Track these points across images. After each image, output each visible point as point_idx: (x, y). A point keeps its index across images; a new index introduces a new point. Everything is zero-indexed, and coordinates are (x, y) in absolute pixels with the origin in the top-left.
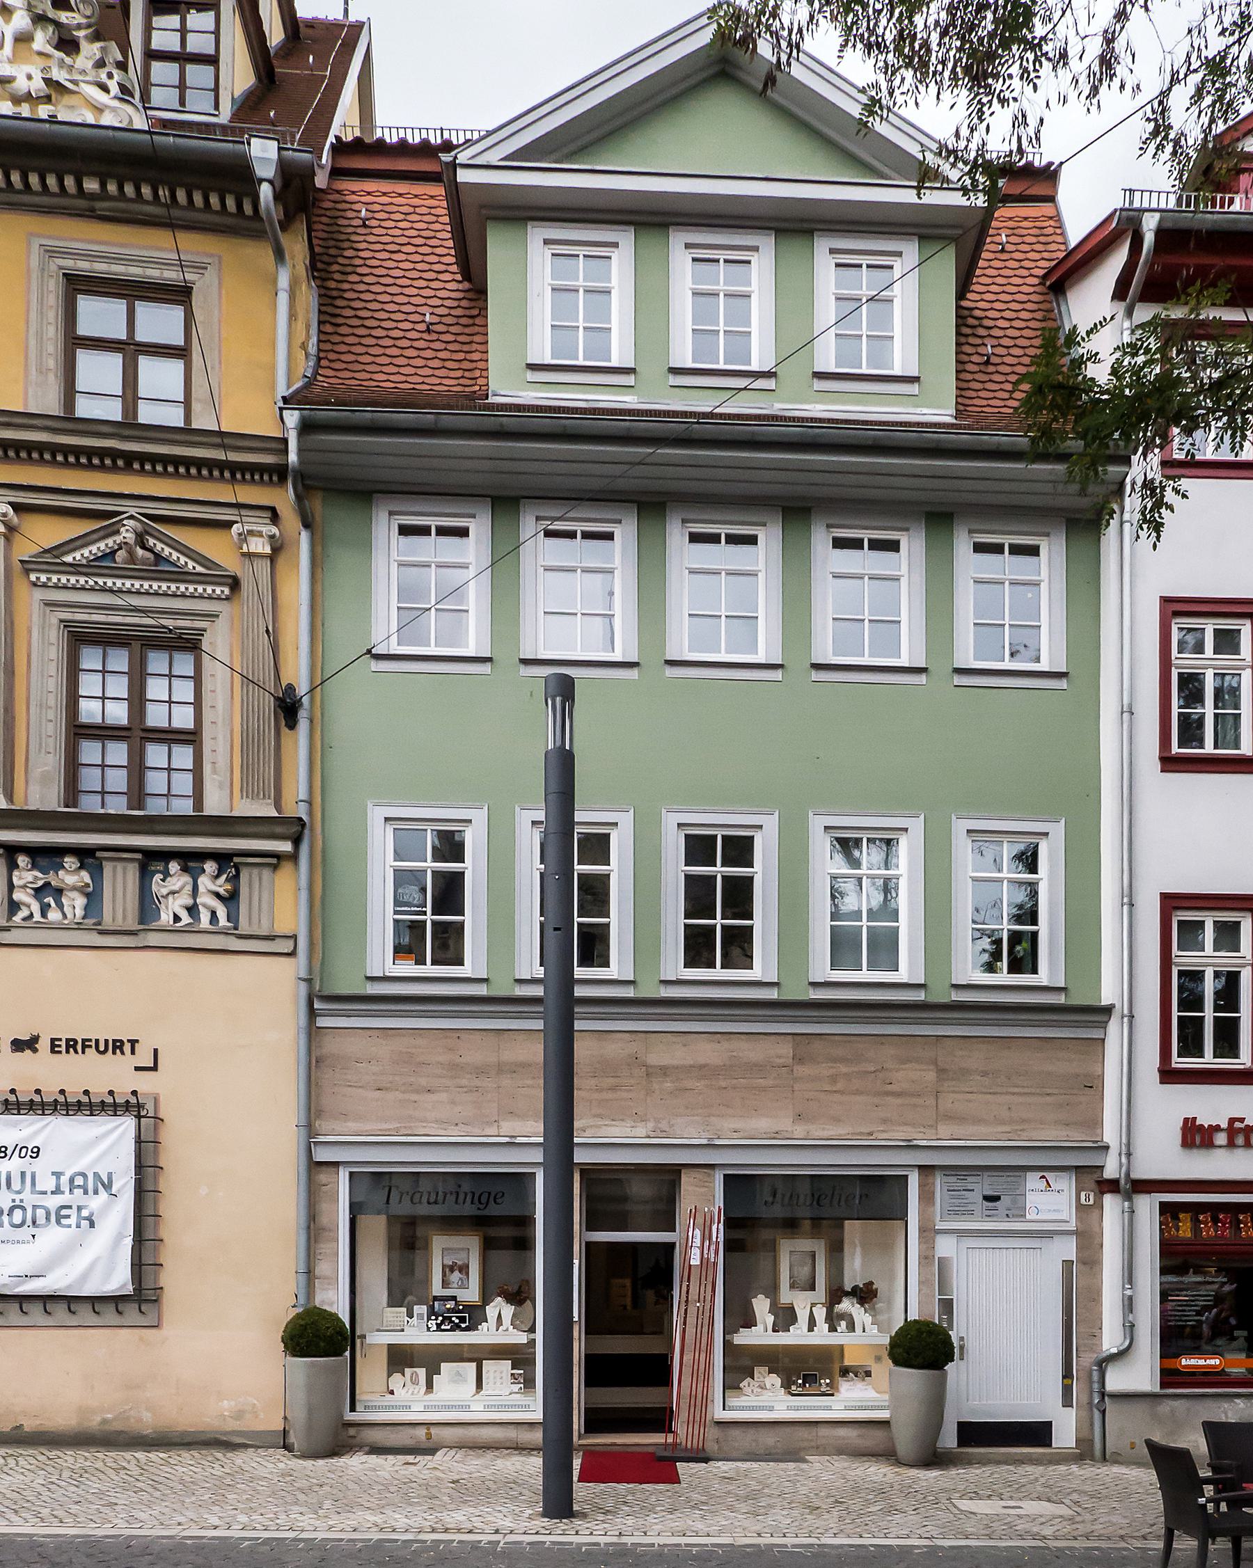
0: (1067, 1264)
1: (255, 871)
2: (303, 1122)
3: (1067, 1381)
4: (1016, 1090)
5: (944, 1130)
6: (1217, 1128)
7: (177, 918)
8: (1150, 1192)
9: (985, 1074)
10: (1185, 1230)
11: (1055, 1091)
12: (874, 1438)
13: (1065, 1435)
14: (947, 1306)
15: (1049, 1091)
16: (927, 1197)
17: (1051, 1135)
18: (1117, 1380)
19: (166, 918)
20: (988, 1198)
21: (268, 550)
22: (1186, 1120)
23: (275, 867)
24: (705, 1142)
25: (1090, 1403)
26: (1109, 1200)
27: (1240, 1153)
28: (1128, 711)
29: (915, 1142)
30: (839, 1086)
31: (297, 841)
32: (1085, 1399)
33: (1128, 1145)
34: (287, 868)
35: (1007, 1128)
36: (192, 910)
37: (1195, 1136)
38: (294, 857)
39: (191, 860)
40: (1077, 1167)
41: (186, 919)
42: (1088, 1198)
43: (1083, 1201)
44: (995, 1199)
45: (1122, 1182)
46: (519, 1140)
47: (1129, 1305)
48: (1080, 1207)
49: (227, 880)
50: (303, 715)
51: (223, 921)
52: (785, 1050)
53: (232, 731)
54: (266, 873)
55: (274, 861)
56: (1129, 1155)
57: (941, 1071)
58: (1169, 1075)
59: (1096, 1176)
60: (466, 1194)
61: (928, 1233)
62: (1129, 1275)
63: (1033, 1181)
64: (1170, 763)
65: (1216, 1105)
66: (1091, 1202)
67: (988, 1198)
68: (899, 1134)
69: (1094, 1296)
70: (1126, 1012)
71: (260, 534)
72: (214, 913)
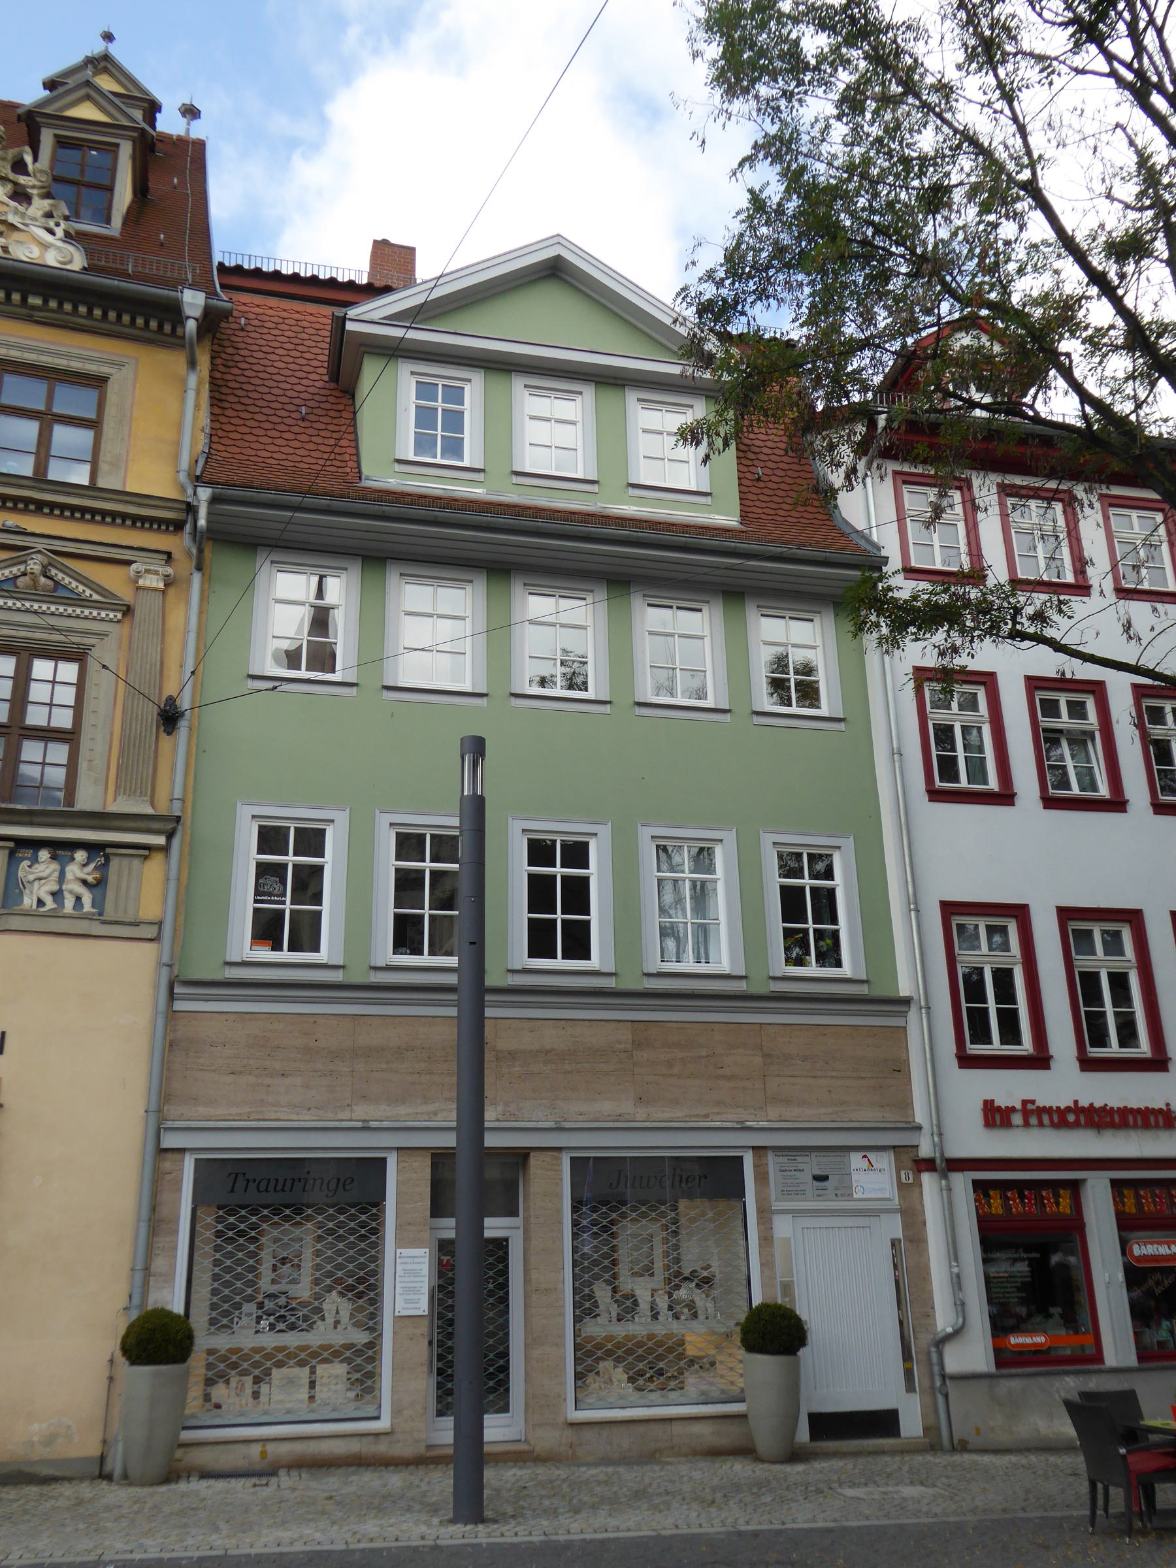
0: (894, 1243)
1: (126, 861)
2: (153, 1107)
3: (908, 1365)
4: (833, 1074)
5: (773, 1112)
6: (1013, 1109)
7: (40, 903)
9: (805, 1059)
10: (996, 1206)
12: (729, 1435)
13: (912, 1425)
14: (787, 1288)
15: (863, 1075)
16: (762, 1177)
17: (867, 1115)
19: (29, 902)
20: (817, 1178)
21: (161, 585)
22: (986, 1102)
23: (146, 858)
24: (552, 1124)
25: (932, 1387)
26: (927, 1178)
28: (897, 753)
30: (676, 1070)
31: (170, 836)
32: (927, 1383)
33: (939, 1126)
34: (157, 860)
36: (57, 895)
38: (165, 849)
39: (61, 849)
40: (894, 1147)
41: (50, 904)
42: (907, 1177)
44: (824, 1178)
45: (938, 1161)
46: (373, 1124)
47: (957, 1282)
48: (901, 1186)
49: (96, 868)
50: (183, 724)
51: (87, 906)
52: (625, 1035)
53: (112, 734)
54: (136, 862)
55: (146, 852)
56: (940, 1135)
57: (767, 1056)
58: (966, 1061)
60: (315, 1180)
61: (765, 1214)
62: (954, 1253)
63: (856, 1160)
64: (935, 795)
65: (1010, 1087)
66: (911, 1181)
67: (817, 1178)
68: (731, 1117)
69: (922, 1274)
70: (923, 1004)
71: (156, 573)
72: (78, 899)
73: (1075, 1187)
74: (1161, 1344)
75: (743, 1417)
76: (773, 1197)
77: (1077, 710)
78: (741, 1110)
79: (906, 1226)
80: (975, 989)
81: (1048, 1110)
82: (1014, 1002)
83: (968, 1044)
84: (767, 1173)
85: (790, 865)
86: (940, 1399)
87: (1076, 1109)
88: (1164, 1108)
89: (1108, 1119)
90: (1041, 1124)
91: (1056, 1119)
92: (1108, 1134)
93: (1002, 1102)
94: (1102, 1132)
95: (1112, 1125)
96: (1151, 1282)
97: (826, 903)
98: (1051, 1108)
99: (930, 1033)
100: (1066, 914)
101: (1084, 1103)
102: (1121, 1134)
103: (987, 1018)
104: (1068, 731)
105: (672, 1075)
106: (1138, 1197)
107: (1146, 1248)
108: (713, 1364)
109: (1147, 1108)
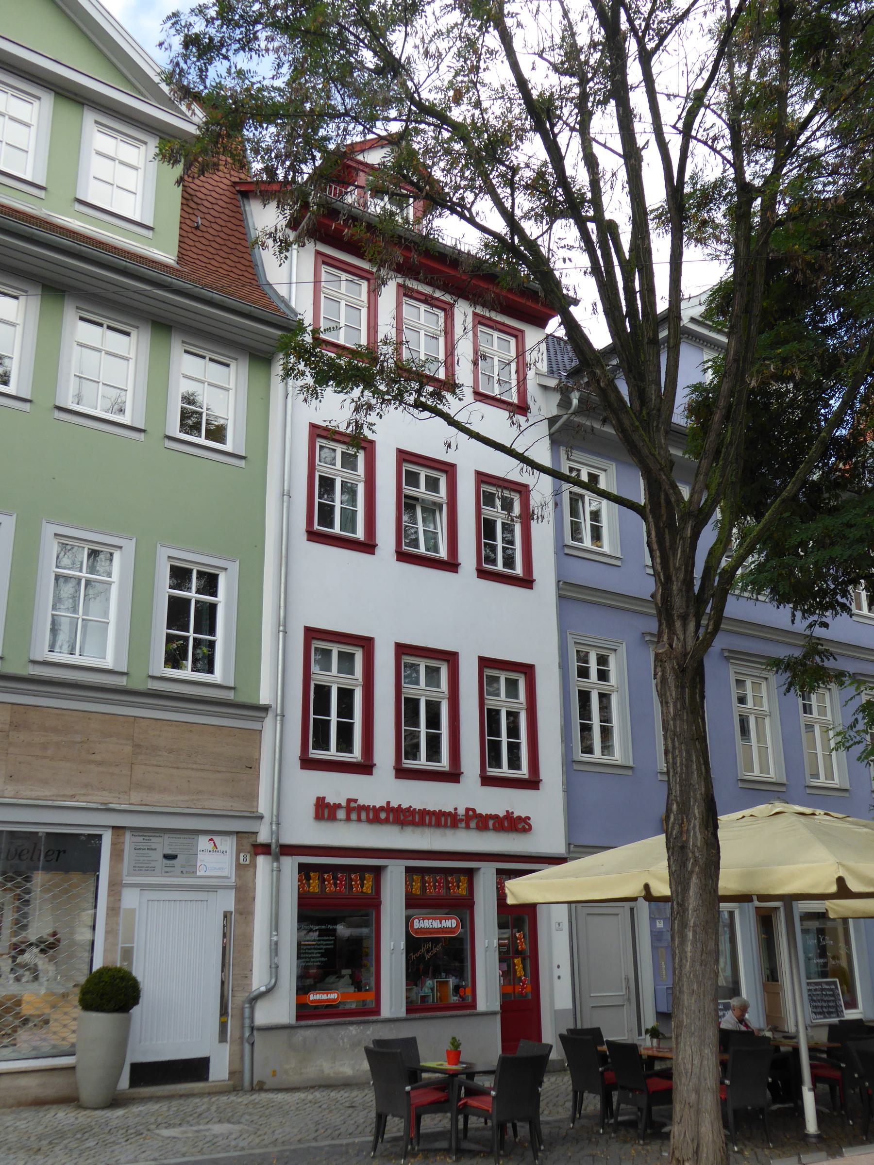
0: (226, 915)
3: (223, 1019)
4: (194, 766)
6: (339, 806)
8: (292, 855)
9: (170, 751)
10: (314, 886)
11: (224, 769)
12: (56, 1086)
13: (219, 1071)
14: (128, 954)
15: (219, 769)
16: (117, 854)
17: (219, 804)
18: (264, 1015)
20: (167, 857)
22: (318, 799)
25: (242, 1037)
27: (354, 827)
28: (286, 495)
29: (111, 806)
30: (50, 752)
32: (237, 1034)
33: (278, 816)
35: (186, 798)
37: (324, 810)
40: (238, 833)
43: (241, 861)
44: (174, 857)
45: (273, 846)
47: (275, 949)
48: (239, 866)
56: (278, 824)
57: (137, 746)
58: (307, 763)
59: (251, 840)
61: (116, 886)
62: (275, 925)
63: (203, 842)
64: (313, 536)
65: (339, 787)
67: (167, 857)
68: (97, 798)
70: (279, 712)
73: (378, 871)
74: (424, 998)
75: (72, 1069)
76: (125, 872)
77: (432, 484)
78: (106, 793)
79: (238, 901)
80: (322, 706)
81: (366, 808)
82: (351, 717)
83: (311, 750)
84: (123, 850)
85: (180, 576)
86: (247, 1047)
87: (388, 809)
88: (453, 812)
89: (410, 818)
90: (359, 820)
91: (371, 816)
92: (409, 830)
93: (331, 800)
94: (404, 828)
95: (413, 823)
96: (423, 950)
97: (207, 617)
98: (369, 806)
99: (281, 737)
100: (402, 649)
101: (394, 804)
102: (419, 830)
103: (329, 728)
104: (423, 500)
105: (45, 757)
106: (423, 882)
107: (426, 923)
108: (47, 1022)
109: (440, 811)
